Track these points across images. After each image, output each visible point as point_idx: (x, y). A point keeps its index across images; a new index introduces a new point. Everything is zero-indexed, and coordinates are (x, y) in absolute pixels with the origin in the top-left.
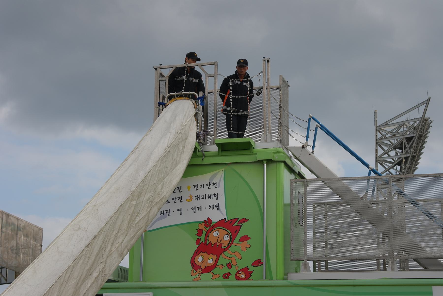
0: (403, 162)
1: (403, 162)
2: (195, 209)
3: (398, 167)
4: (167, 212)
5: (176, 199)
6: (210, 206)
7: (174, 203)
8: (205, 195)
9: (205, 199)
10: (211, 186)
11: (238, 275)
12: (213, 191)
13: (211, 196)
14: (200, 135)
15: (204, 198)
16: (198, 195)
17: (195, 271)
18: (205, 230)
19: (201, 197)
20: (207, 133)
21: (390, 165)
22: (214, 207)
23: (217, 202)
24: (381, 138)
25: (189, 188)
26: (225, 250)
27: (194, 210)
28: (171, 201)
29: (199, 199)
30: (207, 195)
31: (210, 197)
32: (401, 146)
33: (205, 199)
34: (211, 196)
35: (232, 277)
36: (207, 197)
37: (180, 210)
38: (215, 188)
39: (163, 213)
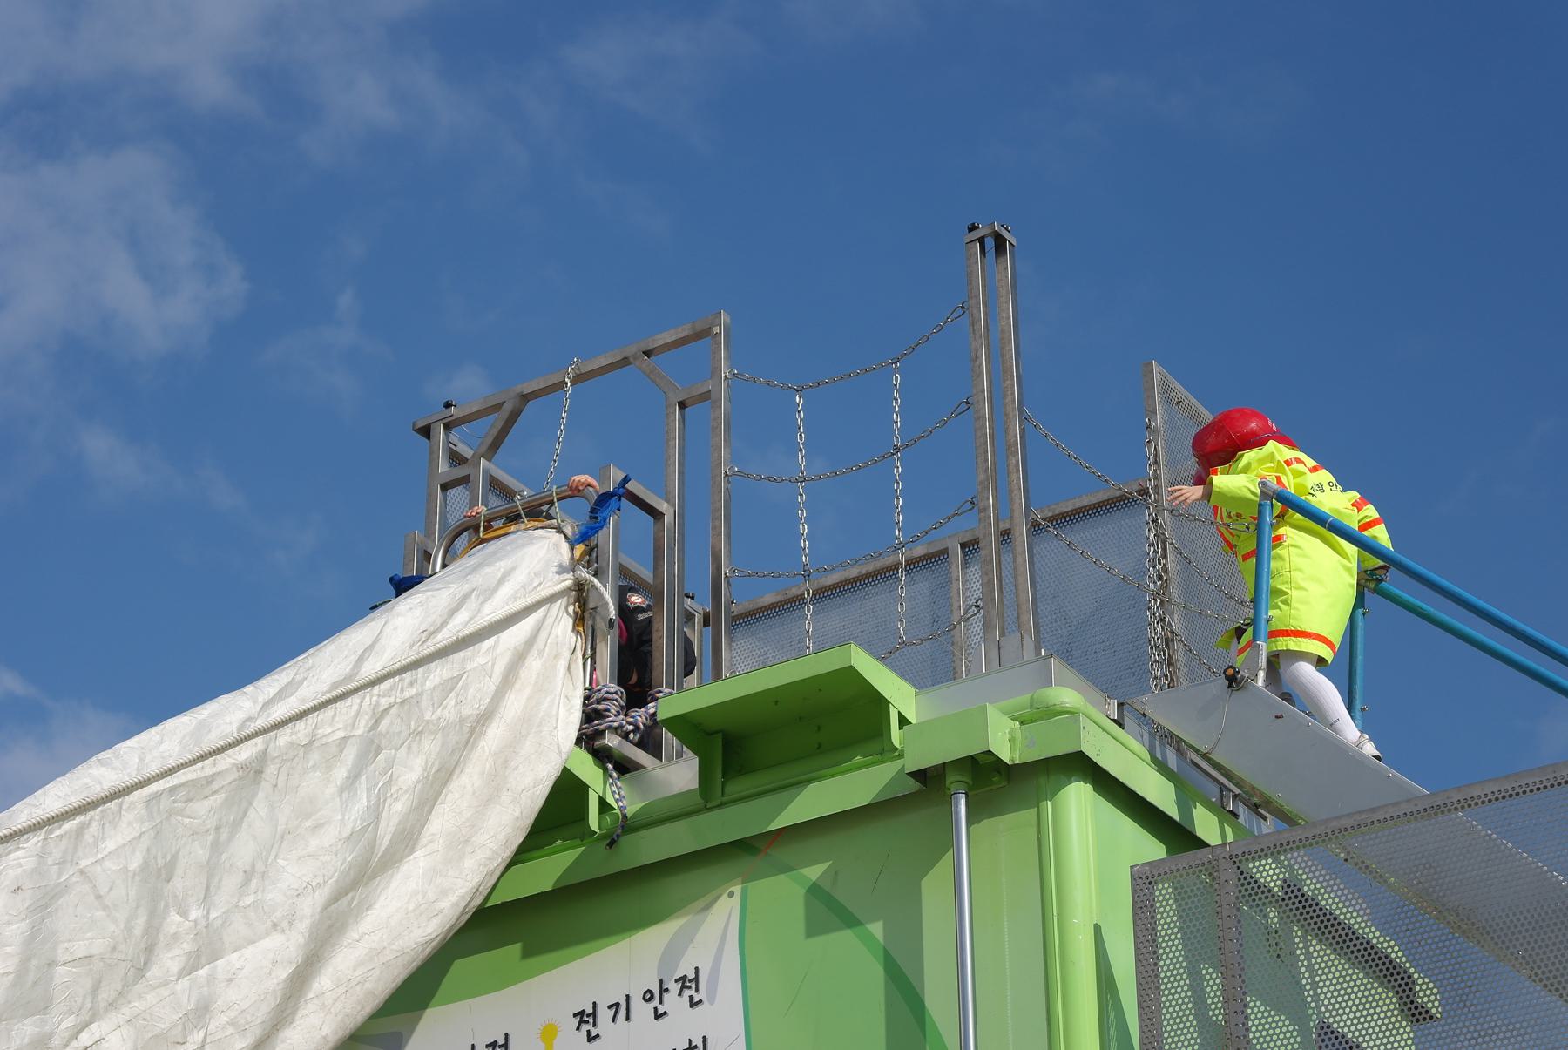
14: (601, 707)
25: (549, 1033)
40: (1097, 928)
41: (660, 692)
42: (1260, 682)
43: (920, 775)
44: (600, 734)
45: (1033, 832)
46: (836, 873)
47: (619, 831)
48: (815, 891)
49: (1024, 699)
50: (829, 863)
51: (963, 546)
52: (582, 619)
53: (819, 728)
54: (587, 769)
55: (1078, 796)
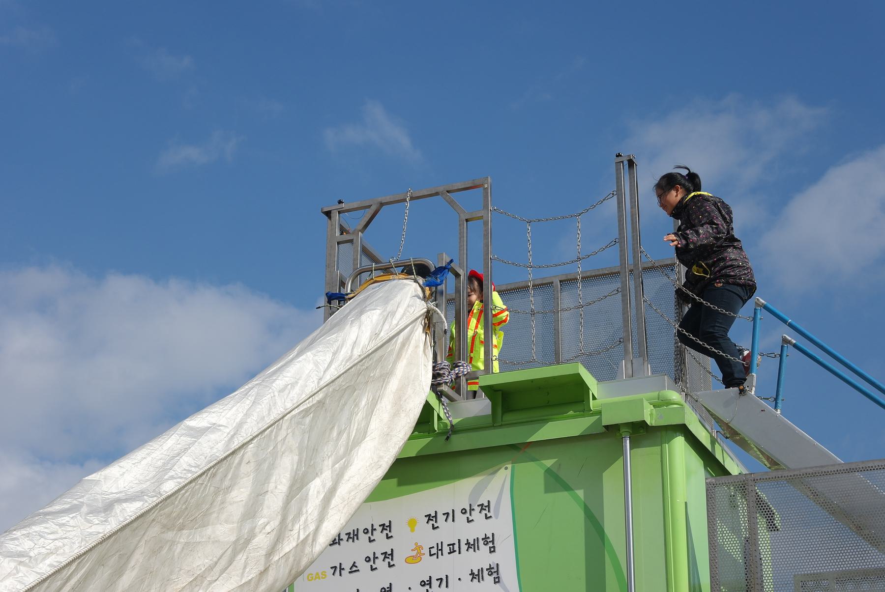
2: (430, 584)
5: (375, 558)
6: (472, 574)
7: (372, 569)
8: (459, 540)
9: (460, 553)
10: (476, 515)
12: (480, 527)
13: (476, 542)
14: (441, 372)
15: (455, 551)
16: (437, 544)
19: (446, 549)
20: (465, 370)
22: (484, 575)
23: (493, 559)
25: (412, 523)
27: (427, 587)
28: (364, 566)
29: (442, 555)
30: (463, 542)
31: (472, 546)
33: (460, 553)
34: (476, 542)
36: (464, 547)
38: (487, 518)
40: (686, 503)
41: (460, 363)
42: (753, 393)
43: (607, 427)
44: (440, 384)
45: (659, 457)
46: (560, 465)
47: (450, 433)
48: (549, 472)
49: (655, 394)
50: (557, 459)
51: (560, 281)
52: (429, 326)
53: (548, 394)
54: (434, 402)
55: (679, 442)
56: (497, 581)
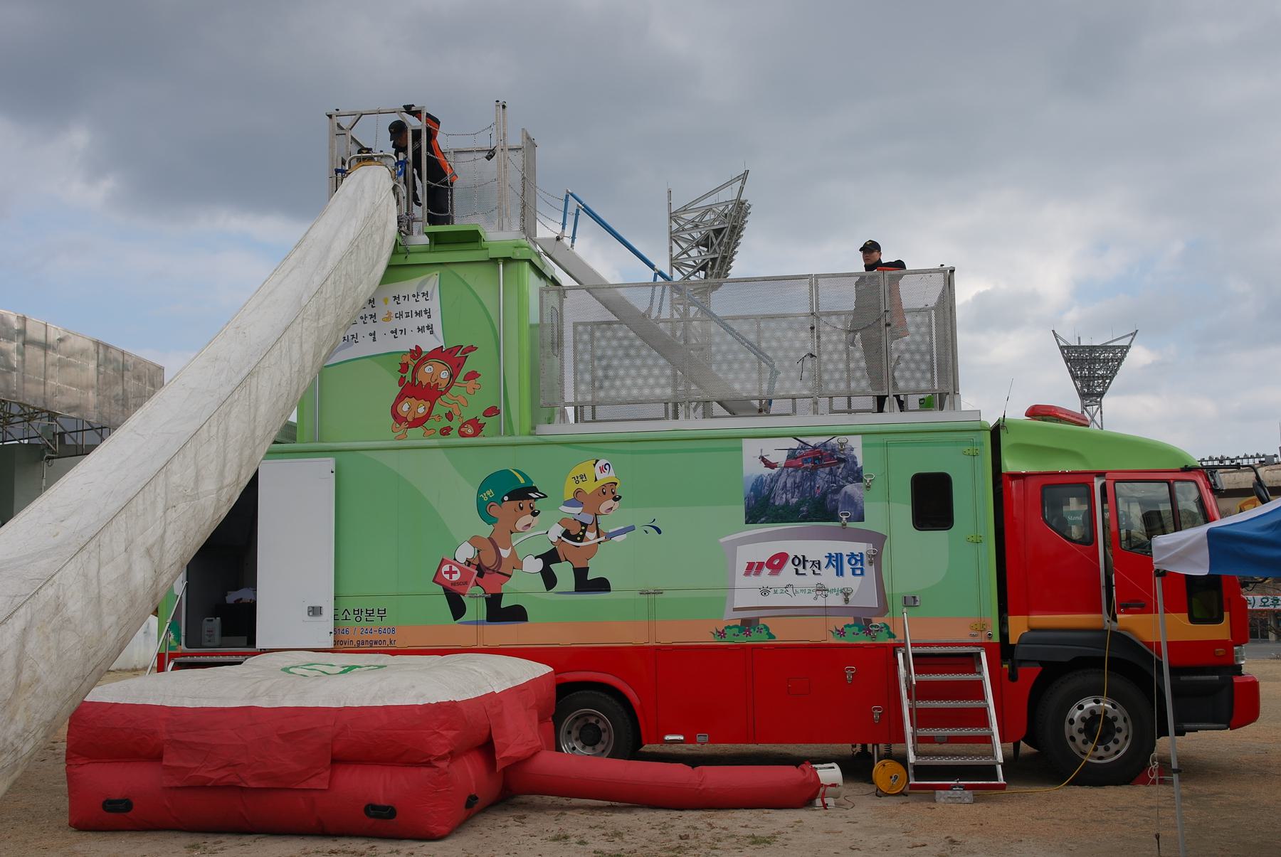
0: (709, 266)
1: (709, 266)
3: (702, 274)
4: (353, 337)
5: (366, 317)
6: (419, 328)
10: (420, 298)
11: (463, 430)
12: (422, 305)
17: (398, 426)
18: (412, 363)
19: (404, 315)
21: (690, 270)
23: (429, 322)
24: (677, 231)
25: (386, 300)
26: (442, 393)
27: (395, 334)
32: (706, 242)
35: (454, 432)
37: (373, 334)
39: (346, 338)
55: (527, 264)
56: (432, 333)
